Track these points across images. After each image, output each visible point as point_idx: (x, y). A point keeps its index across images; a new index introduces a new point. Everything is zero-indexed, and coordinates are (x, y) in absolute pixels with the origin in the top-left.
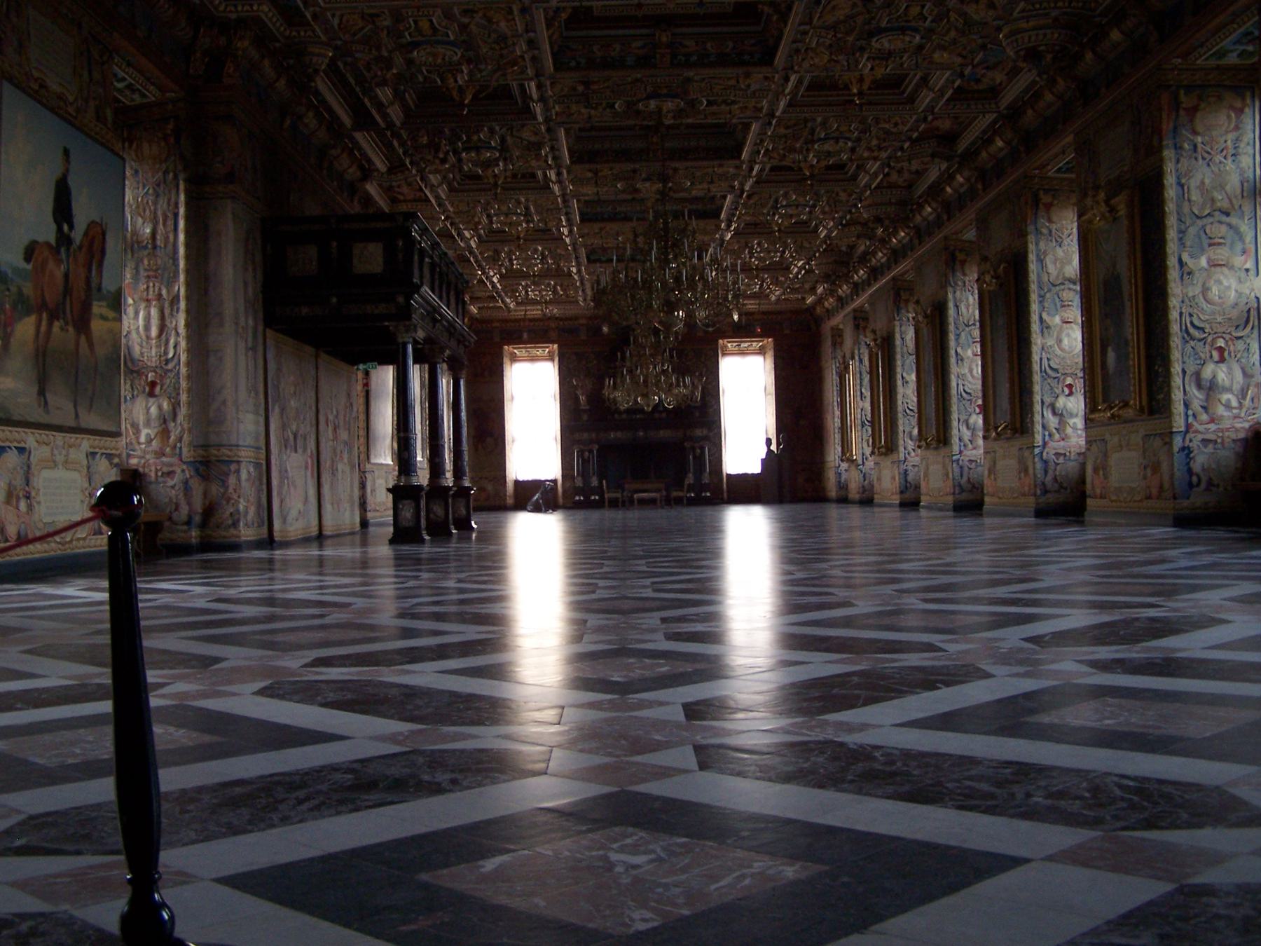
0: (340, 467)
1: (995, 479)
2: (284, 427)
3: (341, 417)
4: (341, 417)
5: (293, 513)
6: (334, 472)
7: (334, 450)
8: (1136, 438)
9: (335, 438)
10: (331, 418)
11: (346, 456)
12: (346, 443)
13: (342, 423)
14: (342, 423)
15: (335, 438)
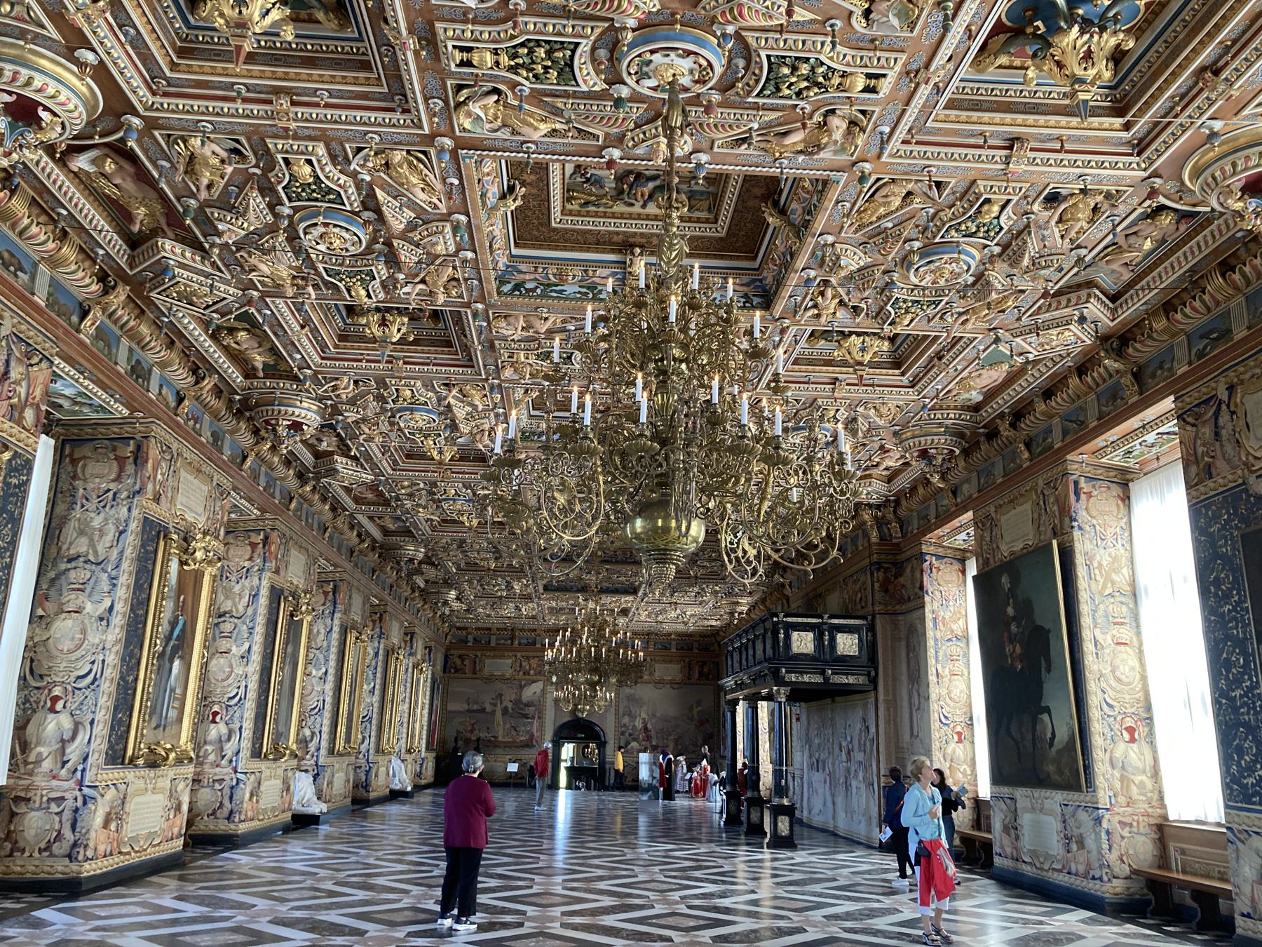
0: (854, 783)
1: (257, 801)
2: (811, 757)
3: (856, 743)
4: (856, 743)
5: (816, 811)
6: (847, 787)
7: (848, 770)
8: (344, 766)
9: (849, 760)
10: (844, 744)
11: (861, 775)
12: (860, 763)
13: (856, 746)
14: (856, 746)
15: (849, 760)
